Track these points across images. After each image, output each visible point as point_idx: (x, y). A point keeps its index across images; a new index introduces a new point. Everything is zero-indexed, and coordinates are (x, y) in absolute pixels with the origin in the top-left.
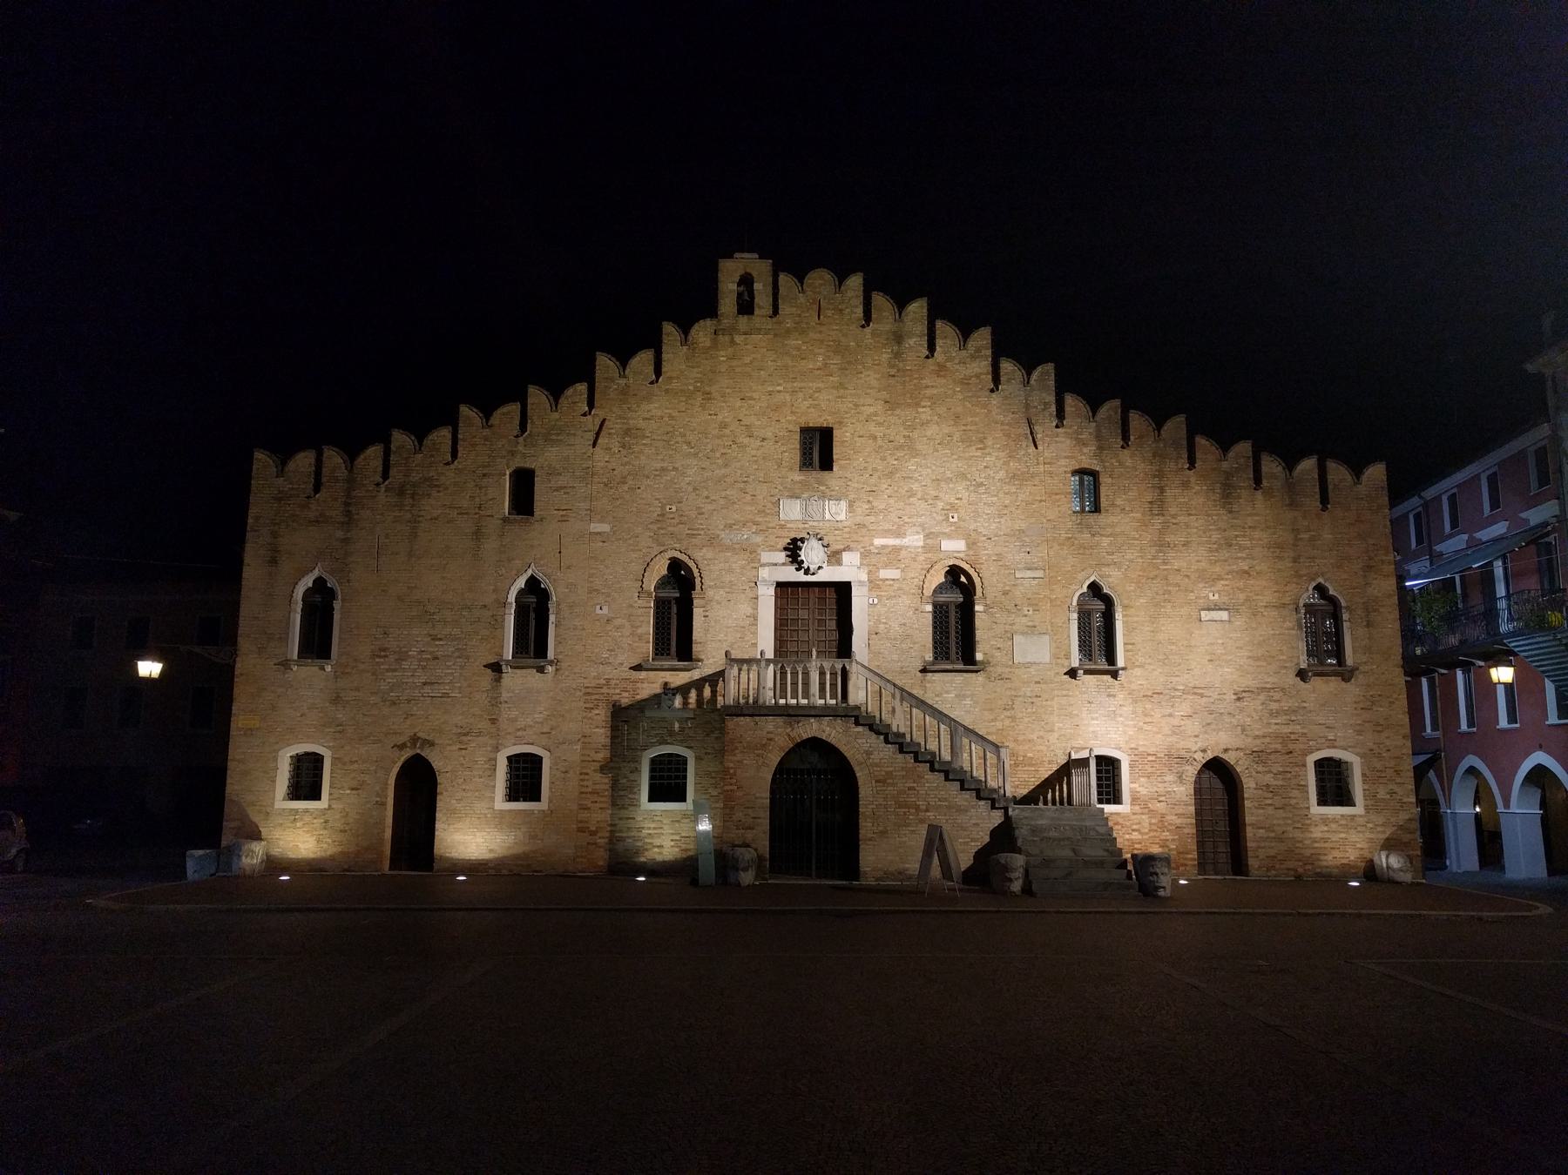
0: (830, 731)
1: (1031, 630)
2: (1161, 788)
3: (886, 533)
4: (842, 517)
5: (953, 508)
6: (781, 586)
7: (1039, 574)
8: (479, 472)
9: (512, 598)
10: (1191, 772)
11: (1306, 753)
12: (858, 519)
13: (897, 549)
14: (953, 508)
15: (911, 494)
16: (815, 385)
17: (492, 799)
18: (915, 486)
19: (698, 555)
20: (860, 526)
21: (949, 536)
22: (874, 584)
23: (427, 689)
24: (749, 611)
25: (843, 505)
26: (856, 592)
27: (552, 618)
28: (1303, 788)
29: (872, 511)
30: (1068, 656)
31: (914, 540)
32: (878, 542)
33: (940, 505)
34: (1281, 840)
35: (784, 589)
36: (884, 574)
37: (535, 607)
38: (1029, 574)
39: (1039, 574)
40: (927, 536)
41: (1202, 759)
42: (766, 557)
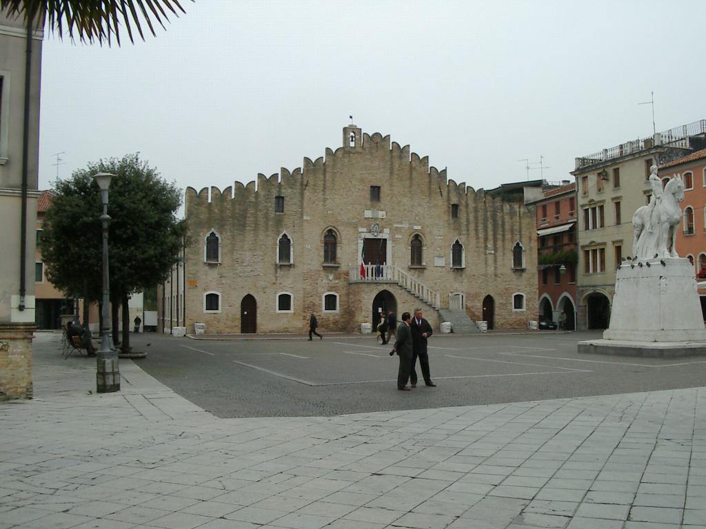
0: (391, 289)
1: (440, 257)
2: (473, 304)
3: (398, 223)
4: (385, 217)
5: (417, 215)
6: (366, 241)
7: (442, 237)
8: (267, 197)
9: (278, 242)
10: (482, 298)
11: (512, 293)
12: (389, 218)
13: (401, 228)
14: (417, 215)
15: (405, 210)
16: (375, 172)
17: (275, 309)
18: (406, 207)
19: (339, 228)
20: (390, 220)
21: (416, 225)
22: (394, 240)
23: (252, 273)
24: (355, 247)
25: (384, 213)
26: (388, 242)
27: (292, 249)
28: (511, 303)
29: (392, 216)
30: (449, 264)
31: (406, 226)
32: (395, 225)
33: (414, 214)
34: (504, 319)
35: (366, 241)
36: (397, 236)
37: (285, 244)
38: (440, 238)
39: (442, 237)
40: (410, 224)
41: (485, 295)
42: (361, 230)
